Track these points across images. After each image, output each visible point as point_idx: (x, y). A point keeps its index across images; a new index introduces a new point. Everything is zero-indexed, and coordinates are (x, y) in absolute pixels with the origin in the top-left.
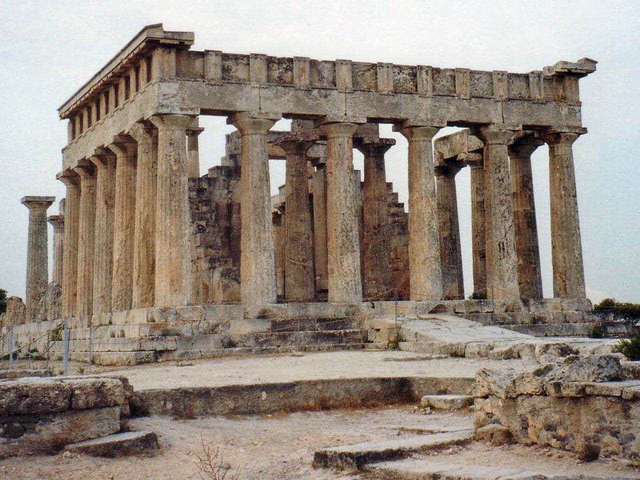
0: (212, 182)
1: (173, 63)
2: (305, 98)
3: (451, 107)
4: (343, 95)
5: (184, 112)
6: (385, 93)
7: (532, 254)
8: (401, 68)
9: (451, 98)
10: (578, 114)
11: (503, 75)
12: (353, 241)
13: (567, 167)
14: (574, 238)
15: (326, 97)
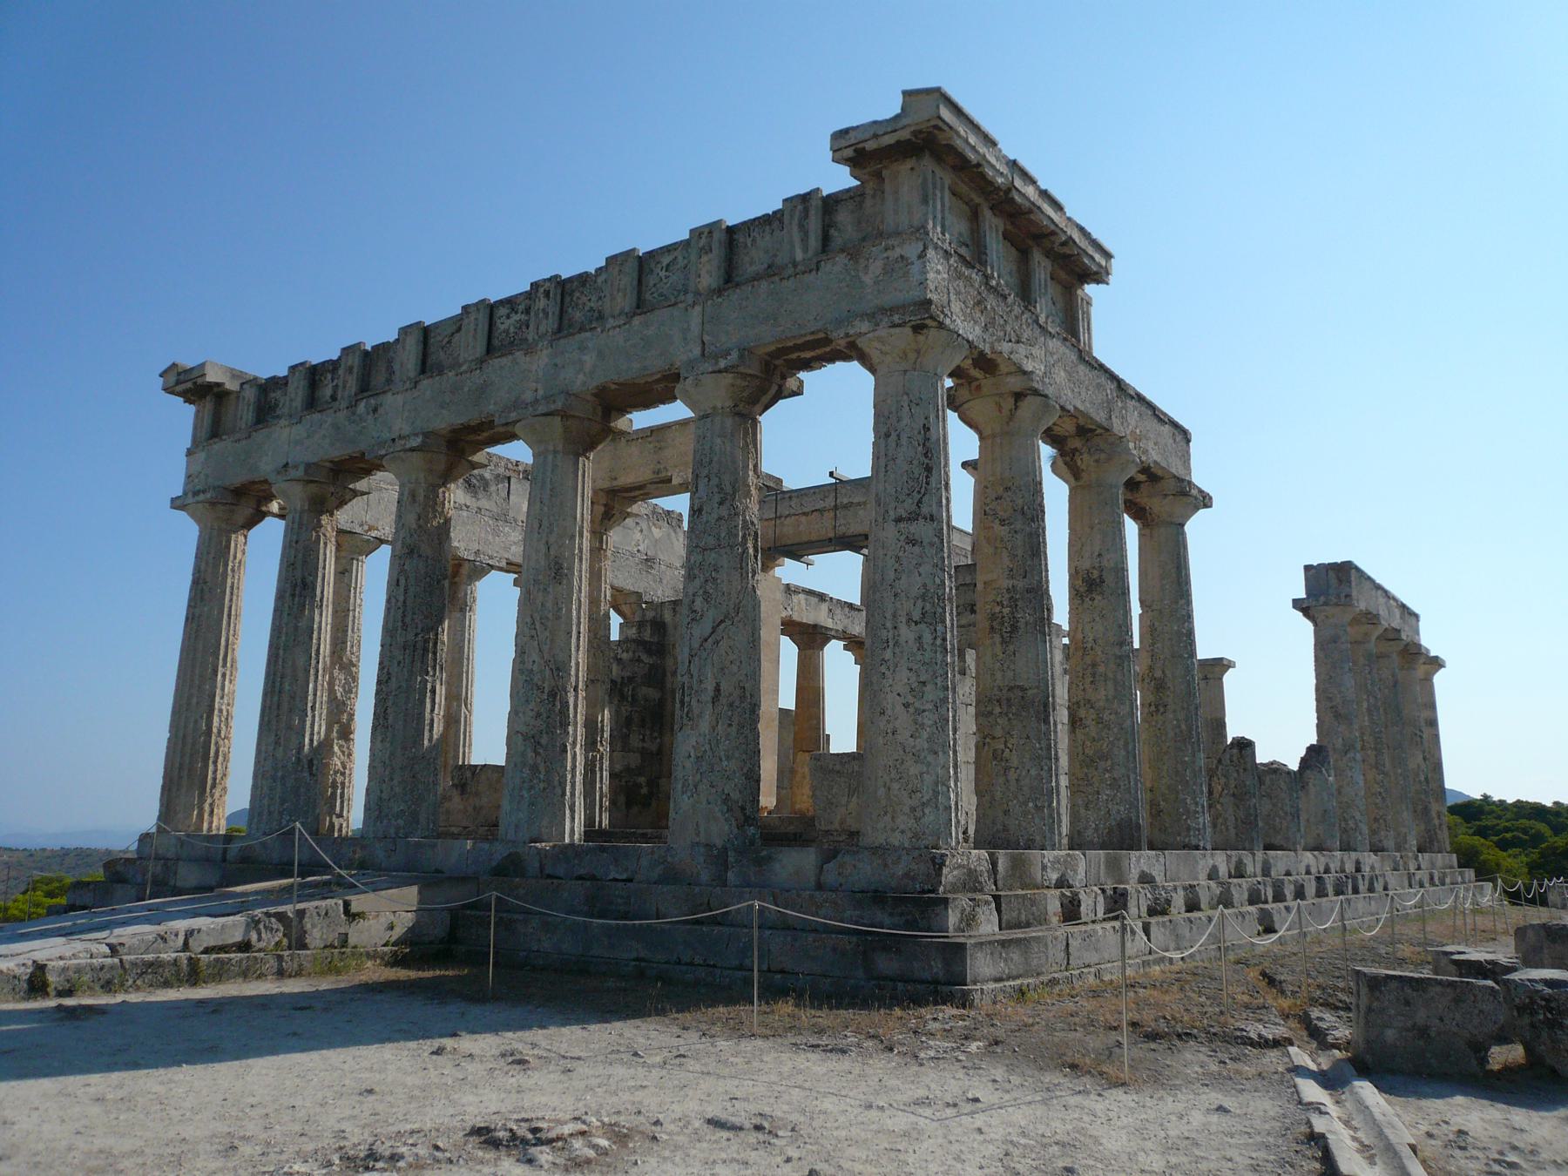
0: (677, 609)
1: (207, 421)
2: (347, 423)
3: (586, 358)
4: (400, 398)
5: (197, 498)
6: (464, 368)
7: (997, 710)
8: (510, 302)
9: (588, 334)
10: (915, 269)
11: (710, 232)
12: (390, 703)
13: (888, 435)
14: (888, 654)
15: (375, 410)
